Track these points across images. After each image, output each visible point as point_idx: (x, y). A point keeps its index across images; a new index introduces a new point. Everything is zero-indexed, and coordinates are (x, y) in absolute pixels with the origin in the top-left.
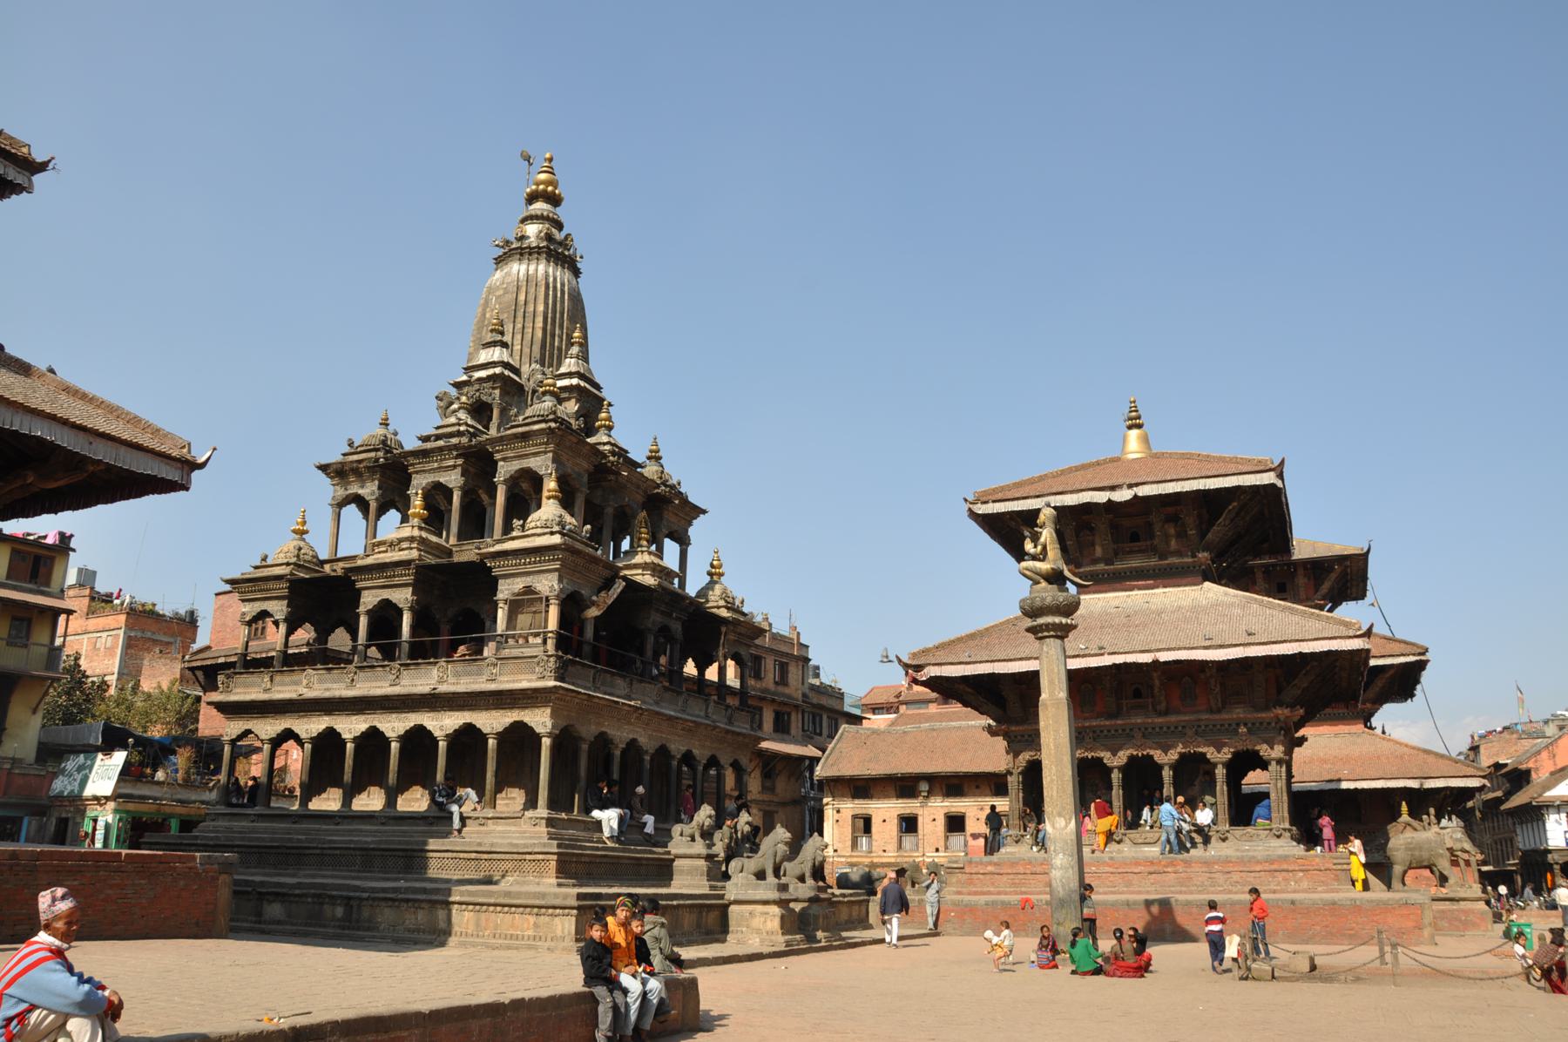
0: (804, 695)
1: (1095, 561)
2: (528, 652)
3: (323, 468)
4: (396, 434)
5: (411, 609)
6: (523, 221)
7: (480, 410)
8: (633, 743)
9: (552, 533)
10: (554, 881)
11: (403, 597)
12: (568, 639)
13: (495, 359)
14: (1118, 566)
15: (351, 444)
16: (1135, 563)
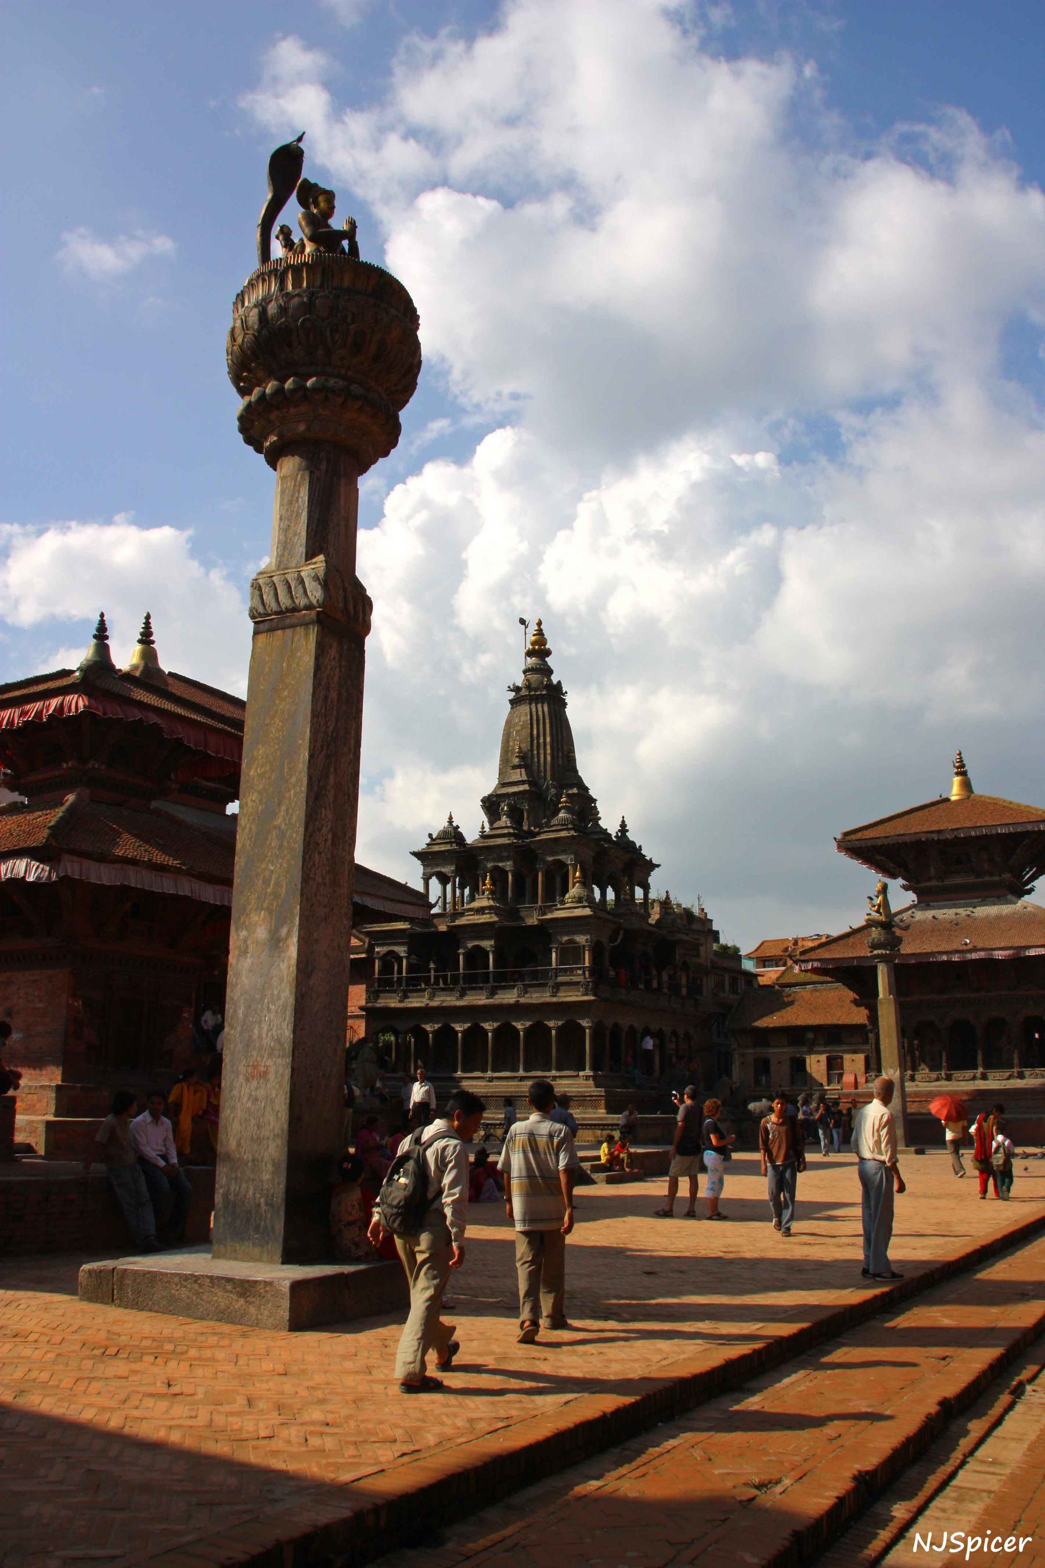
0: (712, 961)
1: (930, 879)
2: (575, 979)
3: (414, 854)
4: (458, 827)
5: (493, 952)
6: (525, 672)
7: (515, 814)
8: (631, 1027)
9: (584, 907)
10: (604, 1111)
11: (487, 944)
12: (597, 971)
13: (525, 778)
14: (947, 882)
15: (430, 836)
16: (958, 880)
